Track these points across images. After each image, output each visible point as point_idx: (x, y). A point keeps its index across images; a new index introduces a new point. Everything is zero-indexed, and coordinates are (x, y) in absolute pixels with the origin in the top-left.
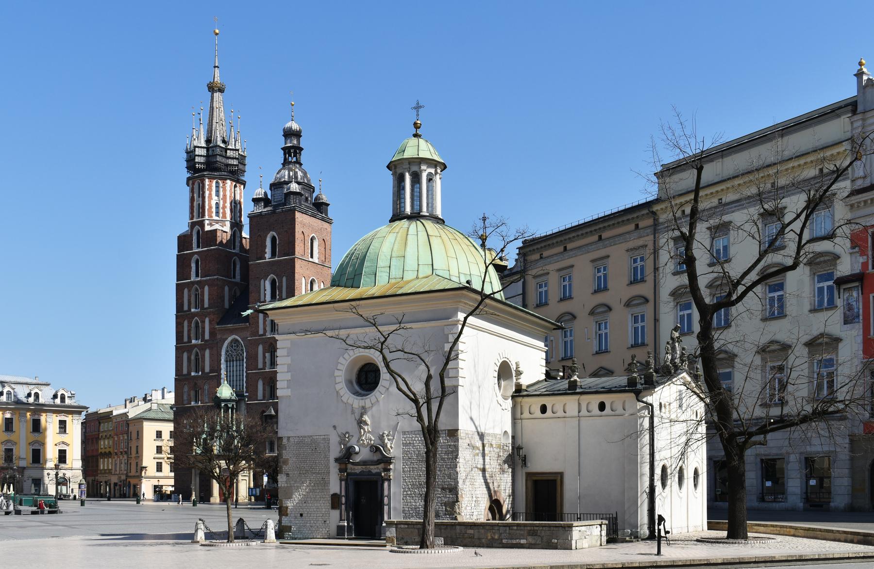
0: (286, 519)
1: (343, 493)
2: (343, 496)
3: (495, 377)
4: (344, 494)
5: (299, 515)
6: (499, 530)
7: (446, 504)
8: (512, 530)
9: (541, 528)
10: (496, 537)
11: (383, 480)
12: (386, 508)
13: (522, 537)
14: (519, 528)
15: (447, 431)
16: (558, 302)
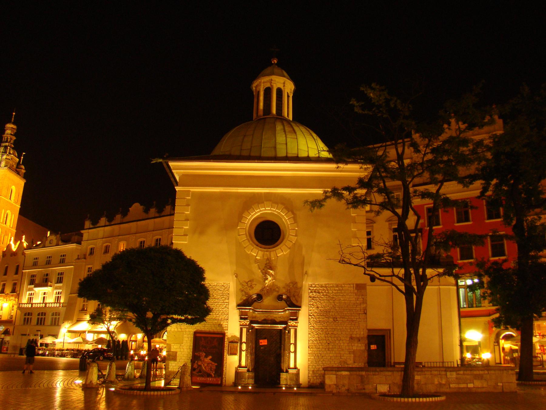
1: (244, 339)
2: (244, 342)
4: (245, 341)
6: (446, 375)
7: (354, 352)
8: (458, 374)
10: (443, 382)
12: (292, 355)
15: (355, 286)
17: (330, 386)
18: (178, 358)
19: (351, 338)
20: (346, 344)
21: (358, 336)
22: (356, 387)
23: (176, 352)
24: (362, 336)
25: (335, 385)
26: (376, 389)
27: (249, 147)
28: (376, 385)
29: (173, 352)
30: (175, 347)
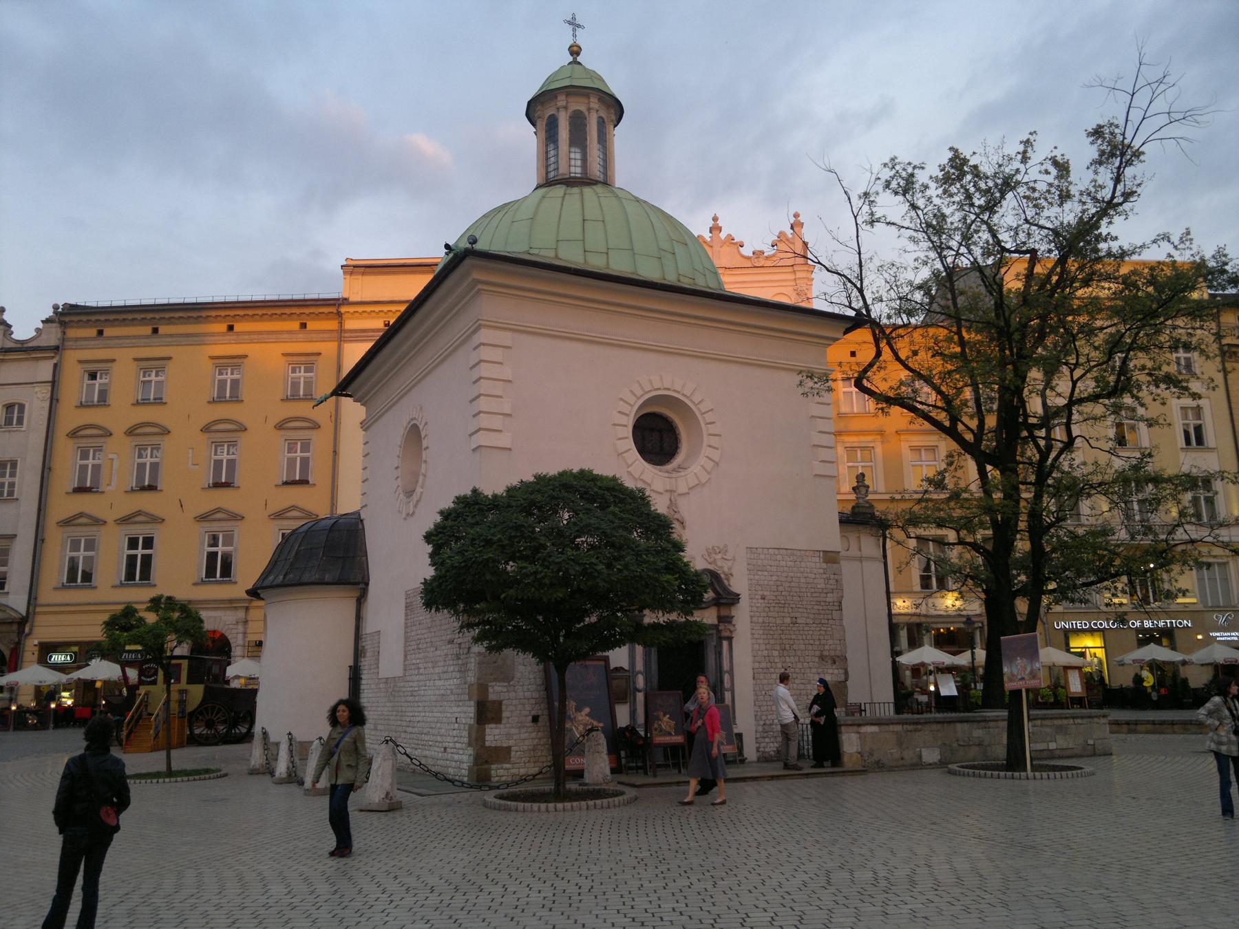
0: (496, 731)
1: (640, 666)
2: (640, 672)
5: (530, 718)
9: (1071, 721)
11: (720, 639)
14: (1044, 722)
16: (132, 404)
17: (851, 755)
18: (505, 714)
19: (822, 658)
20: (814, 670)
21: (832, 653)
22: (889, 755)
23: (500, 703)
25: (859, 753)
26: (920, 757)
27: (604, 250)
28: (920, 751)
29: (494, 702)
30: (498, 689)
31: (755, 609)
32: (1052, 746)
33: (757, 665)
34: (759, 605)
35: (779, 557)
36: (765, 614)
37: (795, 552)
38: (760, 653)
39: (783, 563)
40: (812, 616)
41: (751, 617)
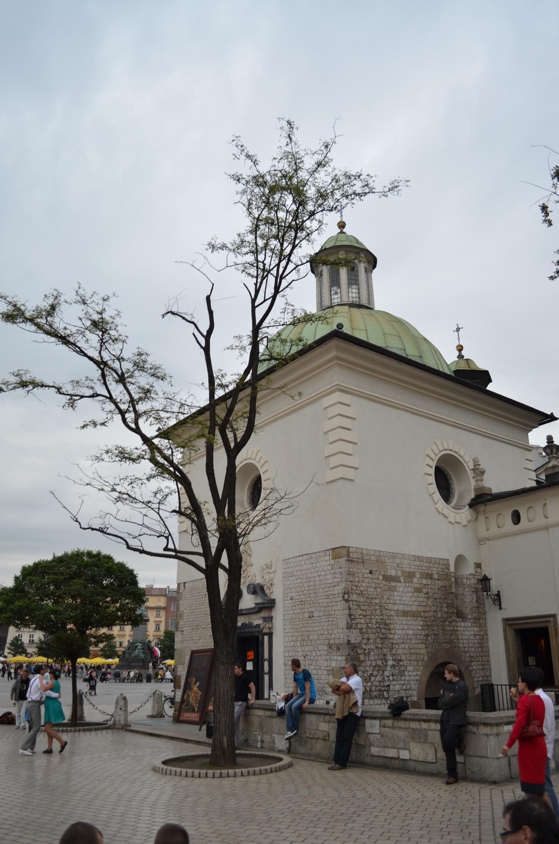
3: (430, 475)
8: (384, 726)
12: (266, 677)
13: (402, 745)
15: (331, 551)
19: (330, 646)
20: (324, 657)
21: (337, 642)
24: (341, 641)
31: (286, 608)
32: (404, 755)
33: (287, 654)
34: (289, 605)
35: (303, 563)
36: (291, 612)
37: (313, 555)
38: (289, 644)
39: (305, 567)
40: (323, 609)
41: (284, 615)
